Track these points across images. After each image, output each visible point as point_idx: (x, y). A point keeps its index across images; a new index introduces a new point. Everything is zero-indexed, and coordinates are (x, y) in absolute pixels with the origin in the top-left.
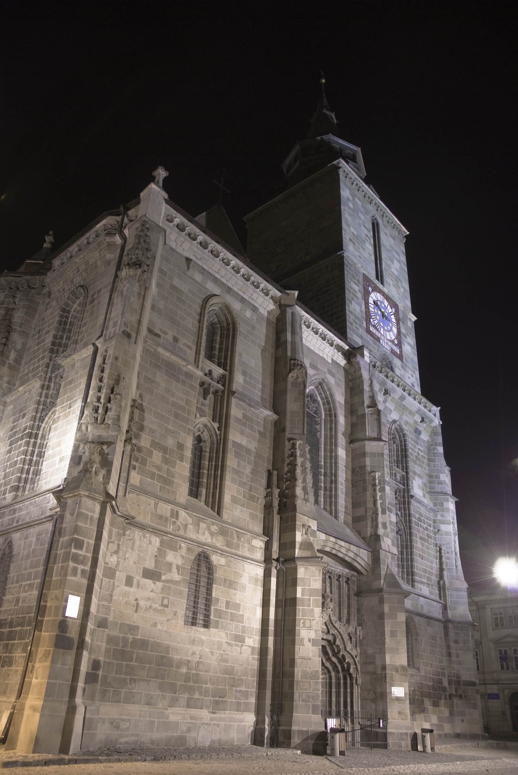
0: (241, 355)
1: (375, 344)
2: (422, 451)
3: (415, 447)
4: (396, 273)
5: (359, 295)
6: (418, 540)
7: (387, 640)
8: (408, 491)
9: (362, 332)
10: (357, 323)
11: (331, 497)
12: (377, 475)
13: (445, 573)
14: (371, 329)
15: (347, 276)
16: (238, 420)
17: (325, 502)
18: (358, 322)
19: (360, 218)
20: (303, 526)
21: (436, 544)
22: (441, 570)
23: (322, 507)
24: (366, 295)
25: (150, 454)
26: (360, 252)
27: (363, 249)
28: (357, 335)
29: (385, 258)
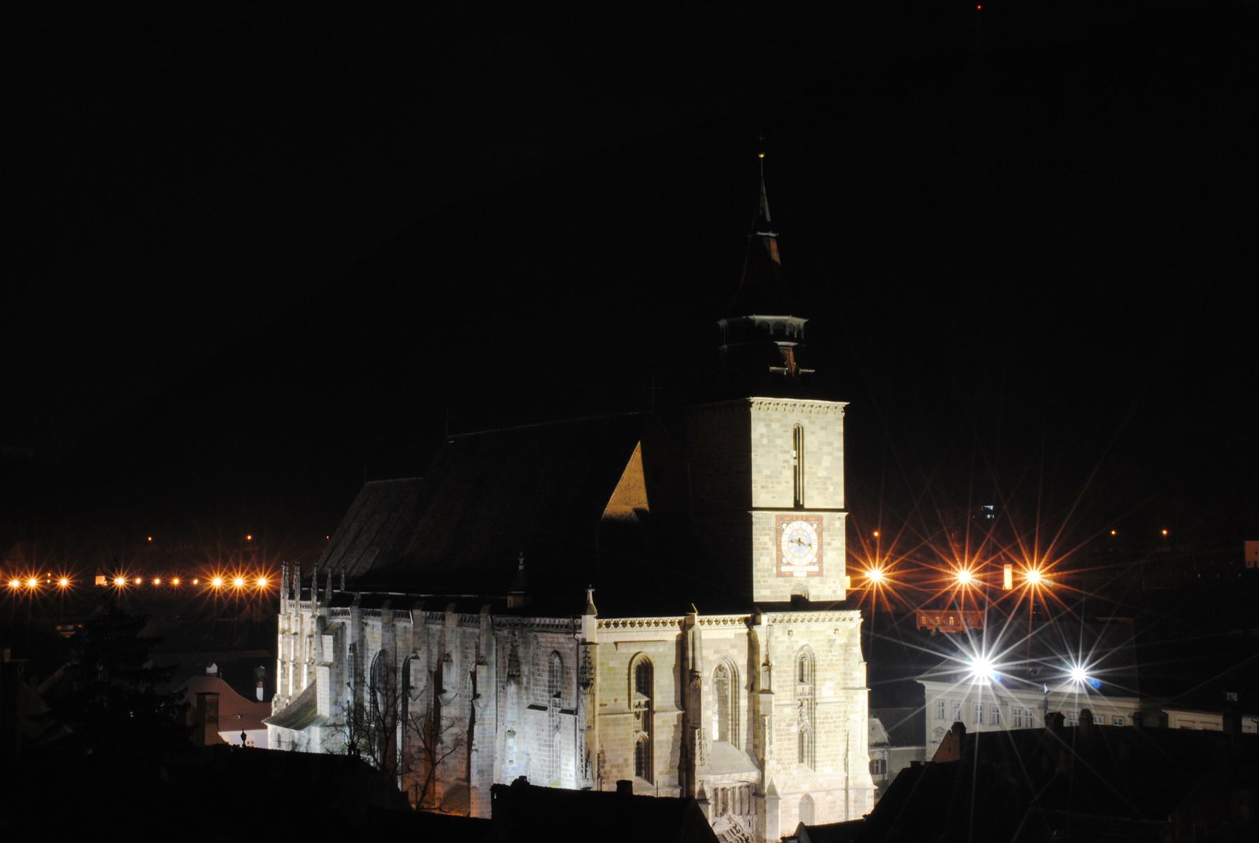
0: (658, 681)
1: (786, 582)
2: (836, 656)
3: (827, 656)
6: (823, 735)
7: (767, 825)
10: (765, 577)
11: (735, 735)
12: (767, 718)
13: (850, 753)
14: (784, 569)
17: (732, 739)
18: (767, 574)
20: (700, 781)
21: (845, 731)
22: (847, 750)
23: (730, 742)
24: (779, 532)
25: (611, 772)
27: (779, 483)
28: (765, 588)
29: (810, 468)
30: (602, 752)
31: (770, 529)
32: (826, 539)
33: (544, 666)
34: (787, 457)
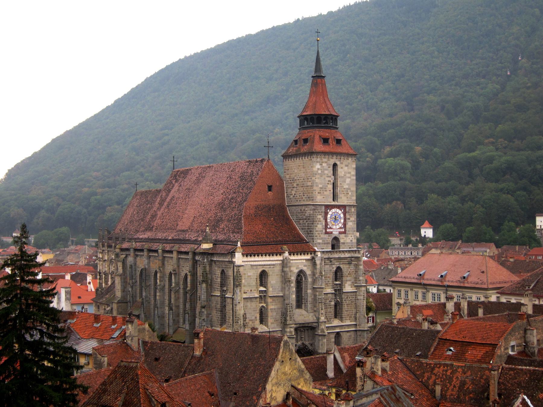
0: (270, 282)
1: (329, 236)
3: (348, 270)
4: (347, 187)
5: (322, 219)
6: (346, 306)
8: (342, 289)
9: (323, 236)
13: (358, 314)
14: (328, 230)
15: (315, 215)
16: (271, 302)
19: (325, 174)
25: (249, 323)
26: (324, 195)
27: (326, 191)
29: (340, 184)
30: (245, 314)
31: (322, 212)
32: (348, 216)
33: (218, 275)
34: (330, 179)
